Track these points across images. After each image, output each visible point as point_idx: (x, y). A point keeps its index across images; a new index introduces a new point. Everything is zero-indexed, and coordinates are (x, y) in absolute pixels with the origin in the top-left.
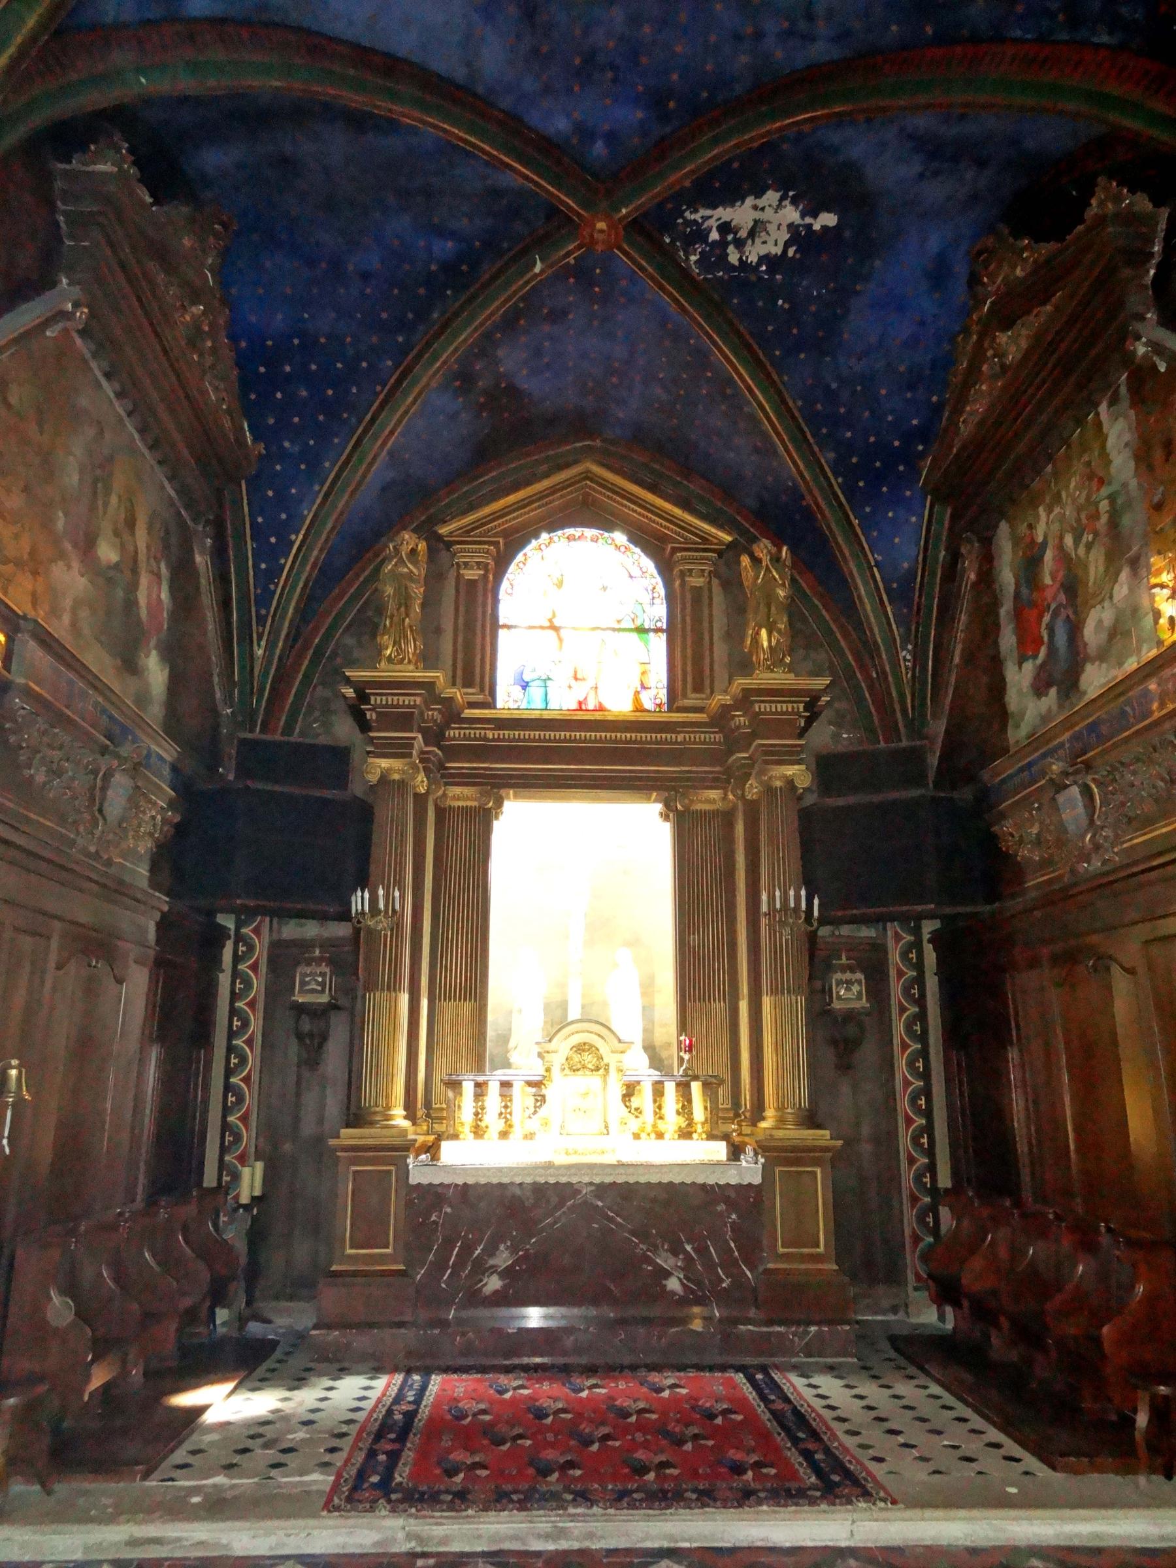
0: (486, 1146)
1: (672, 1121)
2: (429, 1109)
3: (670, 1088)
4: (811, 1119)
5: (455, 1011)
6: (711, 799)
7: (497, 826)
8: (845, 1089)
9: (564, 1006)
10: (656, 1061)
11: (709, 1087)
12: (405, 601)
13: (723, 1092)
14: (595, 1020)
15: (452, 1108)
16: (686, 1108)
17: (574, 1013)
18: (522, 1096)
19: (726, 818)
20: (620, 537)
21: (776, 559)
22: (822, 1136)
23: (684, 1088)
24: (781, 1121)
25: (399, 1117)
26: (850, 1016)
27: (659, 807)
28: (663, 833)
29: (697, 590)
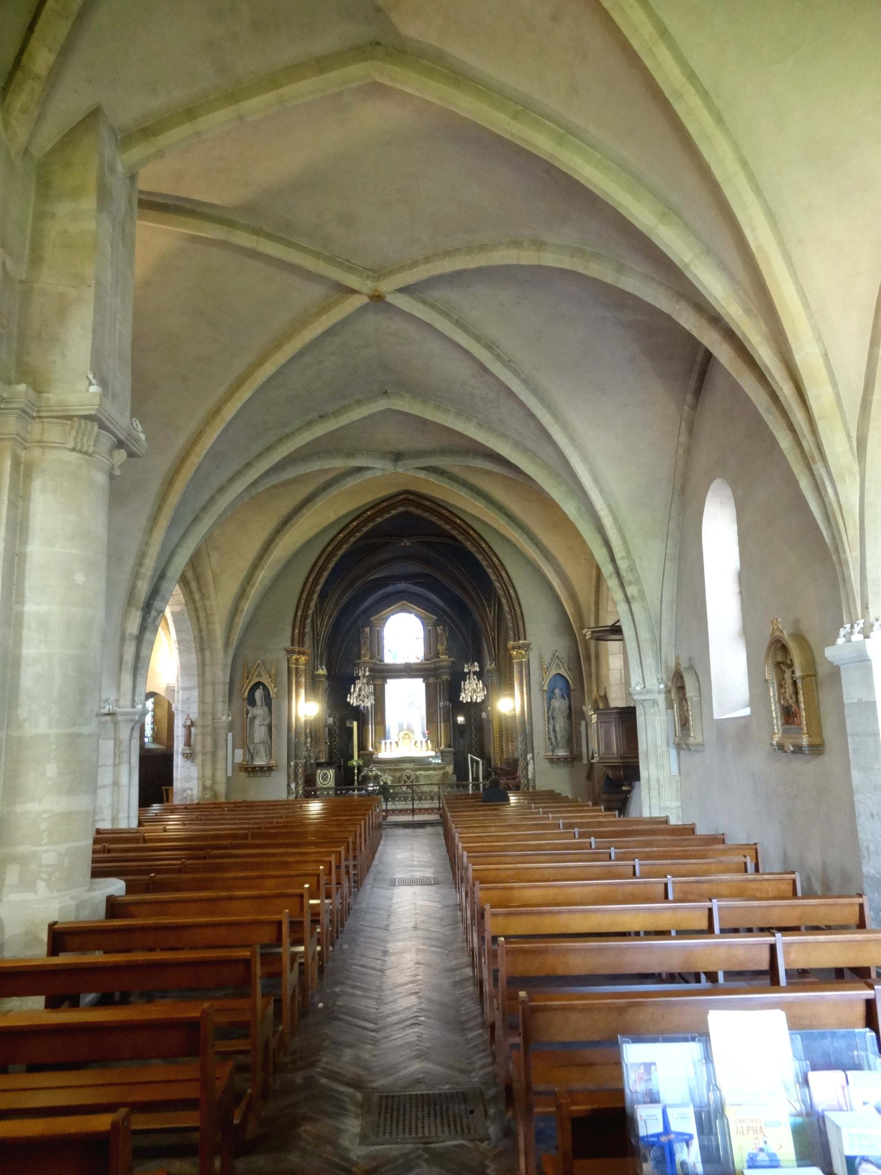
0: (386, 752)
1: (424, 748)
2: (376, 748)
3: (424, 743)
4: (450, 746)
5: (380, 727)
6: (432, 680)
7: (387, 686)
8: (462, 741)
9: (402, 724)
10: (424, 737)
11: (431, 741)
12: (365, 643)
13: (435, 742)
14: (409, 729)
15: (380, 747)
16: (427, 746)
17: (405, 727)
18: (394, 745)
19: (436, 683)
20: (413, 615)
21: (444, 630)
22: (450, 749)
23: (426, 742)
24: (445, 747)
25: (370, 749)
26: (461, 725)
27: (422, 680)
28: (424, 685)
29: (429, 630)
